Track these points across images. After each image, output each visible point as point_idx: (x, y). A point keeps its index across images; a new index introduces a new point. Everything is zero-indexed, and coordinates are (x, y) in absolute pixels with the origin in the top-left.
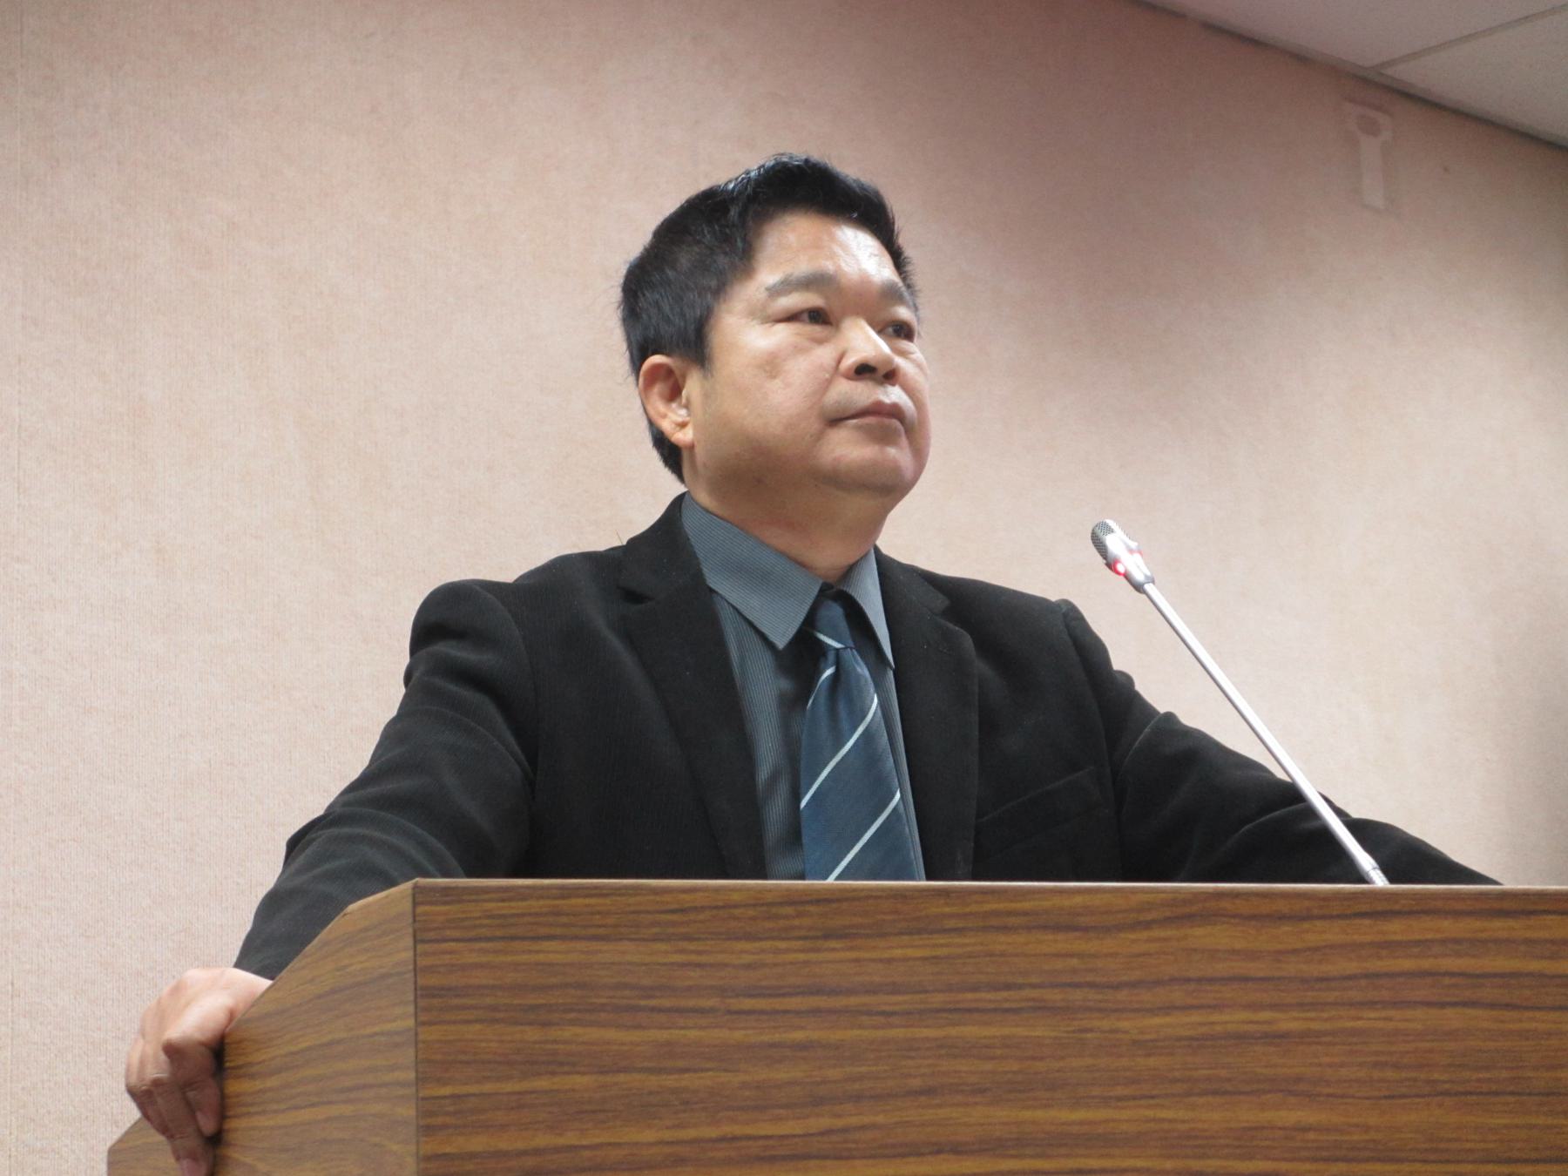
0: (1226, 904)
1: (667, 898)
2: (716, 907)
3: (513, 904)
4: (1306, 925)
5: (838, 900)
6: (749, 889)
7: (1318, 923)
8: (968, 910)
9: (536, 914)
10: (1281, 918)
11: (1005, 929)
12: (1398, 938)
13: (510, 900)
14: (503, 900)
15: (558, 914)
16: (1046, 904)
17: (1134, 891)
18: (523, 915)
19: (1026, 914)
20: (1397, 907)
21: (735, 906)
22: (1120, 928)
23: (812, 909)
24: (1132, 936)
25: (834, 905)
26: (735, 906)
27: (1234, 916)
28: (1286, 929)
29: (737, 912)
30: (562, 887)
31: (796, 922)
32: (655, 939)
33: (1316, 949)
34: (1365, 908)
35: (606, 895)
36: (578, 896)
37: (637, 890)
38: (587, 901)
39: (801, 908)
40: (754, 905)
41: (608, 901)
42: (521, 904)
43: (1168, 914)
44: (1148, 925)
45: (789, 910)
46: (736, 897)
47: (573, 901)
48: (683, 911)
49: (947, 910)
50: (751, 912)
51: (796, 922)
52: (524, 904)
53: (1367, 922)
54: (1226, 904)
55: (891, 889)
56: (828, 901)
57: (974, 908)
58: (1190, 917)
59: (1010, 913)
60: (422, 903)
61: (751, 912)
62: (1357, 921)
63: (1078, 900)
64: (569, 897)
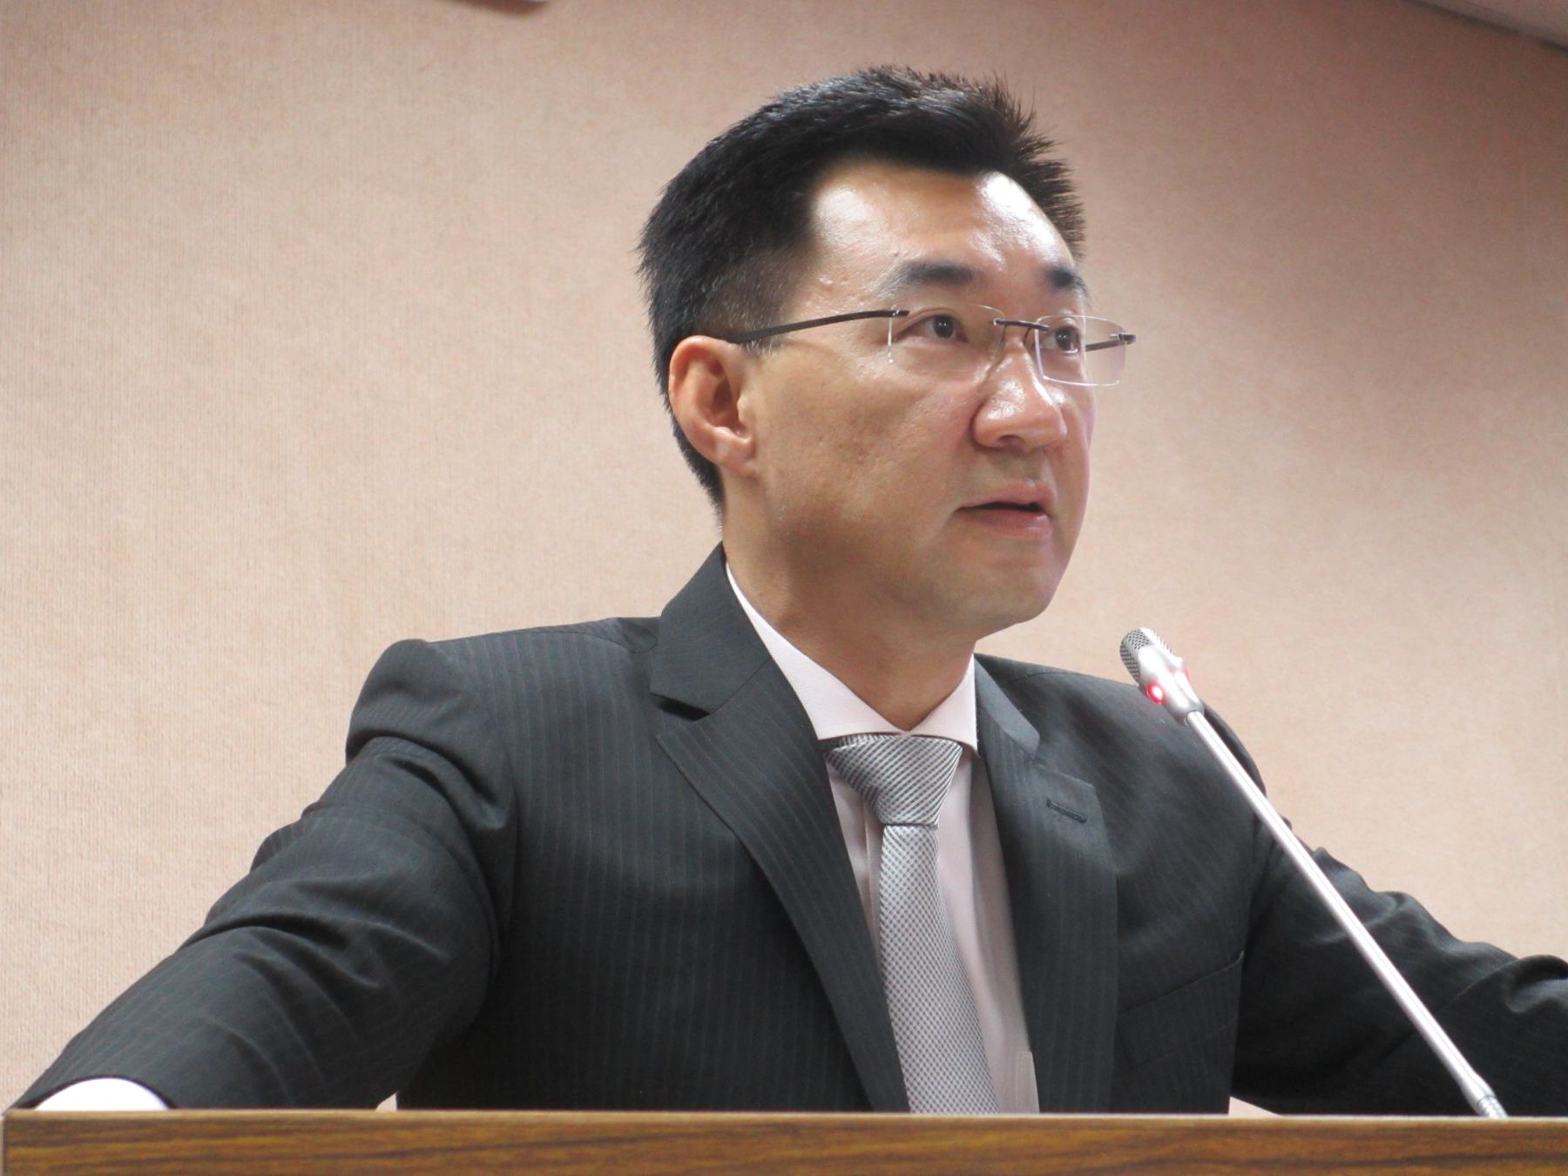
0: (1213, 1145)
1: (378, 1136)
2: (452, 1150)
3: (152, 1145)
5: (633, 1140)
6: (502, 1124)
8: (826, 1153)
9: (187, 1160)
13: (149, 1138)
14: (137, 1140)
15: (216, 1158)
16: (945, 1144)
17: (1075, 1126)
18: (166, 1160)
19: (912, 1158)
20: (1468, 1149)
21: (480, 1147)
23: (593, 1151)
25: (626, 1147)
26: (480, 1147)
27: (1225, 1162)
29: (483, 1155)
30: (220, 1122)
34: (1425, 1151)
35: (288, 1132)
36: (245, 1134)
37: (335, 1125)
39: (576, 1151)
40: (509, 1147)
41: (291, 1140)
42: (166, 1145)
43: (1126, 1159)
45: (559, 1154)
46: (480, 1135)
48: (402, 1154)
49: (797, 1153)
50: (504, 1156)
52: (173, 1143)
54: (1213, 1145)
55: (713, 1124)
56: (618, 1140)
57: (836, 1150)
59: (890, 1158)
60: (15, 1145)
61: (504, 1156)
64: (234, 1134)
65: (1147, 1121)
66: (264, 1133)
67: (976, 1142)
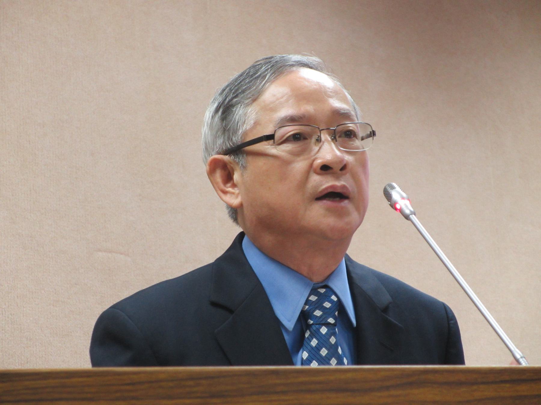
4: (475, 387)
7: (482, 386)
10: (461, 384)
11: (310, 391)
12: (525, 393)
16: (332, 378)
19: (320, 383)
20: (524, 377)
21: (161, 381)
22: (371, 390)
23: (204, 382)
24: (379, 394)
28: (465, 389)
31: (195, 389)
32: (118, 399)
33: (480, 400)
38: (80, 380)
44: (387, 388)
47: (74, 380)
48: (133, 384)
49: (278, 381)
50: (171, 384)
51: (195, 389)
53: (508, 385)
56: (213, 378)
58: (411, 384)
61: (171, 384)
62: (503, 385)
63: (349, 375)
65: (406, 368)
66: (82, 377)
67: (343, 377)
